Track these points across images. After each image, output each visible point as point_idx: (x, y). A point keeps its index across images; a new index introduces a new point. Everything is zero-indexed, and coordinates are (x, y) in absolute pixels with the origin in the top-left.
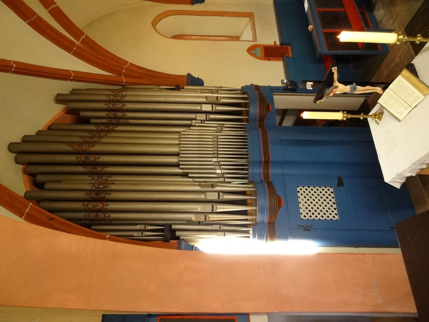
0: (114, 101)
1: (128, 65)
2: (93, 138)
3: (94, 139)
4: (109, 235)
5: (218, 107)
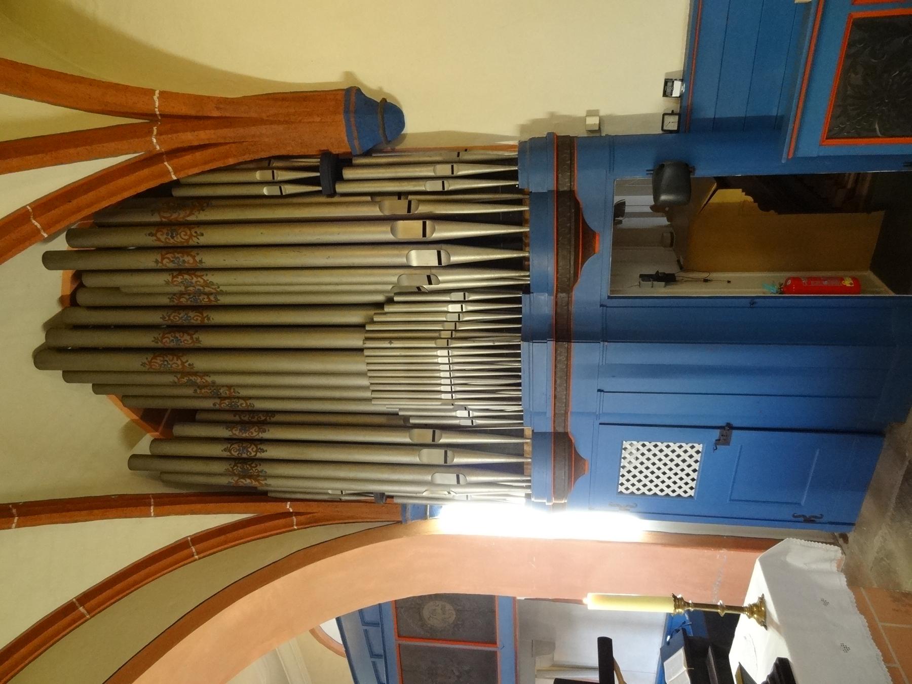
0: (181, 271)
1: (157, 104)
2: (181, 342)
3: (183, 343)
4: (289, 503)
5: (441, 275)
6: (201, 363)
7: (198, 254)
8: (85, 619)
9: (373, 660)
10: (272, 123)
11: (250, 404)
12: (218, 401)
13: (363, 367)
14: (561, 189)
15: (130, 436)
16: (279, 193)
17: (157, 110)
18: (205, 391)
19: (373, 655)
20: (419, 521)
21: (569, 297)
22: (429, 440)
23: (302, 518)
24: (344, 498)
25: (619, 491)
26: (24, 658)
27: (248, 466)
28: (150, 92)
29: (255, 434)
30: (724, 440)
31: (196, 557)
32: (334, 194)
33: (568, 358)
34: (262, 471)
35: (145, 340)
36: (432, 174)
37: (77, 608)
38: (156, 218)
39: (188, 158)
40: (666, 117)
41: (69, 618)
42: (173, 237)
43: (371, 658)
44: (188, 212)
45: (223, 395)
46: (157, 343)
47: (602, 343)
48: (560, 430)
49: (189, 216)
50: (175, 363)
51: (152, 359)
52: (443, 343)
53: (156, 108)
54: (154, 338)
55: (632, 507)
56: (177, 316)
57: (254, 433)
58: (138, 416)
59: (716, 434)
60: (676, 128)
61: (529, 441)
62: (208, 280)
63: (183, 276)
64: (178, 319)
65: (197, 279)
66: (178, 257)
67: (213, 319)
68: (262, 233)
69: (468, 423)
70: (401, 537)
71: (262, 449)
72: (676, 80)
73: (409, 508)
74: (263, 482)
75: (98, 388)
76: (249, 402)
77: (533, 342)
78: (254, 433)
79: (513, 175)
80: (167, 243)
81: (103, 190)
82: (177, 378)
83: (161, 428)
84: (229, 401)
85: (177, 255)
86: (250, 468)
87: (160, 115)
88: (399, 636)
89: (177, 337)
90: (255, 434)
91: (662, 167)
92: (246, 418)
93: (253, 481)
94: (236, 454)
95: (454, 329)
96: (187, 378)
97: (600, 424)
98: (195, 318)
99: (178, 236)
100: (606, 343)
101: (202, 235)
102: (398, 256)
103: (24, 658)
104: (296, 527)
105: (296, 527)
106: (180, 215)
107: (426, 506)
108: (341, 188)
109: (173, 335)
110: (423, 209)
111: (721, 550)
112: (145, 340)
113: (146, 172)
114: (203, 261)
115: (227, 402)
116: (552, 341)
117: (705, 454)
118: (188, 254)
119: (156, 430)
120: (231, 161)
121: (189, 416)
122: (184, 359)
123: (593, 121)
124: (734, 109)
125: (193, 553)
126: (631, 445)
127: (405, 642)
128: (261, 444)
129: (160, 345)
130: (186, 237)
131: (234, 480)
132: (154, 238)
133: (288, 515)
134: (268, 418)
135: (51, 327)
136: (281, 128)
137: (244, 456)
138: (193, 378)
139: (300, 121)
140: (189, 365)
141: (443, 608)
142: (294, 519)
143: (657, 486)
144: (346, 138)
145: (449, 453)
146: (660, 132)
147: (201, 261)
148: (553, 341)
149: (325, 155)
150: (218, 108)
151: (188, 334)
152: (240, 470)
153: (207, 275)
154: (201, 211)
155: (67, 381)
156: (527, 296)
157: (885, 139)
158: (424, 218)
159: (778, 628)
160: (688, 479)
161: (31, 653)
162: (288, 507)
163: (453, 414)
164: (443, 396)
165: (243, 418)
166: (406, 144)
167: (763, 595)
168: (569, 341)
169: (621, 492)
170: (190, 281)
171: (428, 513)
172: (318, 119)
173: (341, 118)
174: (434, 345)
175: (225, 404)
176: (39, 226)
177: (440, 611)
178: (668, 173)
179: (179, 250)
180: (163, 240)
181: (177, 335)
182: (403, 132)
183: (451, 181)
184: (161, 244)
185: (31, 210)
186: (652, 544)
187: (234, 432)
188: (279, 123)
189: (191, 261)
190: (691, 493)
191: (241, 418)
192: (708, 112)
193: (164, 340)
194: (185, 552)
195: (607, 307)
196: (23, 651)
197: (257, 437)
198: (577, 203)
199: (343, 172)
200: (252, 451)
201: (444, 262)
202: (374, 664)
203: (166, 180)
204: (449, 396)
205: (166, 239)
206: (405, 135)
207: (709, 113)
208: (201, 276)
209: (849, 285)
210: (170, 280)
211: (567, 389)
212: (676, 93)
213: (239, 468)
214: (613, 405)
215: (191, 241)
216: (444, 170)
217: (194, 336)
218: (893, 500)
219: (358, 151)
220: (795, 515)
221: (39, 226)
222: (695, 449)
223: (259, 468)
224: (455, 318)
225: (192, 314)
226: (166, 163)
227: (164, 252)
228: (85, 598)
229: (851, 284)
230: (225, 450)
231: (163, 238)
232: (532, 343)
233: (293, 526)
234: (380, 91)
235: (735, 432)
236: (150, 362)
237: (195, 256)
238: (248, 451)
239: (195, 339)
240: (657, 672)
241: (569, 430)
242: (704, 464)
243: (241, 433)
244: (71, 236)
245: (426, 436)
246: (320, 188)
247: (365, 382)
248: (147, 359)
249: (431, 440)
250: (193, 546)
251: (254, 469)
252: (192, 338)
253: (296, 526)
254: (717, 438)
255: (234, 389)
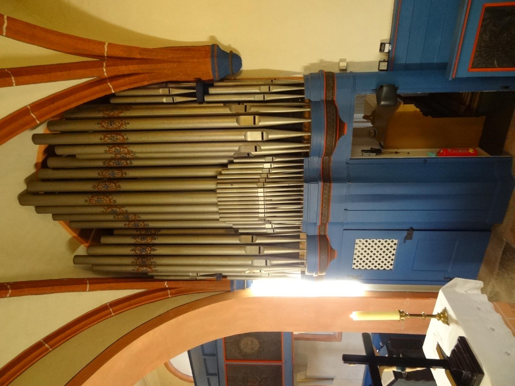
0: (114, 145)
1: (106, 50)
2: (109, 187)
3: (110, 188)
4: (166, 282)
5: (262, 146)
6: (120, 200)
7: (125, 135)
8: (48, 351)
9: (208, 377)
10: (171, 62)
11: (146, 224)
12: (127, 223)
13: (215, 200)
14: (327, 99)
15: (72, 245)
16: (172, 101)
17: (105, 53)
18: (120, 217)
19: (208, 374)
20: (240, 290)
21: (330, 159)
22: (250, 241)
23: (173, 291)
24: (198, 278)
25: (353, 268)
26: (14, 374)
27: (145, 259)
28: (103, 44)
29: (149, 241)
30: (409, 237)
31: (113, 314)
32: (203, 102)
33: (329, 192)
34: (153, 262)
35: (88, 187)
36: (258, 91)
37: (44, 345)
38: (101, 115)
39: (121, 81)
40: (381, 63)
41: (38, 351)
42: (111, 125)
43: (207, 375)
44: (120, 111)
45: (131, 219)
46: (95, 188)
47: (348, 183)
48: (322, 233)
49: (120, 113)
50: (105, 200)
51: (92, 197)
52: (261, 185)
53: (105, 52)
54: (93, 185)
55: (359, 276)
56: (107, 173)
57: (149, 240)
58: (76, 234)
59: (405, 233)
60: (386, 69)
61: (305, 240)
62: (130, 150)
63: (115, 148)
64: (107, 174)
65: (124, 149)
66: (113, 136)
67: (128, 174)
68: (163, 123)
69: (271, 231)
70: (231, 299)
71: (155, 249)
72: (386, 43)
73: (235, 282)
74: (154, 269)
75: (56, 217)
76: (145, 223)
77: (311, 183)
78: (149, 240)
79: (301, 92)
80: (107, 128)
81: (72, 98)
82: (105, 209)
83: (90, 242)
84: (134, 222)
85: (113, 135)
86: (146, 260)
87: (107, 57)
88: (226, 360)
89: (107, 185)
90: (149, 241)
91: (382, 87)
92: (143, 232)
93: (148, 268)
94: (138, 252)
95: (266, 177)
96: (111, 209)
97: (344, 230)
98: (118, 174)
99: (114, 124)
100: (350, 183)
101: (128, 123)
102: (240, 135)
103: (14, 374)
104: (170, 296)
105: (170, 296)
106: (115, 113)
107: (244, 281)
108: (207, 99)
109: (105, 184)
110: (253, 110)
111: (407, 299)
112: (88, 187)
113: (97, 88)
114: (128, 138)
115: (132, 223)
116: (321, 182)
117: (399, 245)
118: (120, 135)
119: (87, 243)
120: (146, 83)
121: (110, 232)
122: (110, 198)
123: (343, 65)
124: (415, 59)
125: (111, 312)
126: (360, 241)
127: (228, 363)
128: (153, 246)
129: (96, 189)
130: (119, 125)
131: (136, 268)
132: (100, 125)
133: (166, 289)
134: (156, 232)
135: (29, 181)
136: (175, 65)
137: (144, 253)
138: (114, 209)
139: (186, 62)
140: (114, 201)
141: (252, 341)
142: (169, 291)
143: (373, 264)
144: (211, 72)
145: (262, 248)
146: (377, 70)
147: (127, 139)
148: (322, 182)
149: (198, 81)
150: (140, 54)
151: (114, 183)
152: (141, 261)
153: (129, 147)
154: (128, 111)
155: (38, 213)
156: (307, 158)
157: (499, 68)
158: (254, 114)
159: (456, 322)
160: (389, 260)
161: (18, 371)
162: (166, 284)
163: (263, 226)
164: (260, 215)
165: (141, 232)
166: (242, 76)
167: (445, 308)
168: (330, 182)
169: (354, 268)
170: (119, 150)
171: (245, 286)
172: (196, 60)
173: (209, 60)
174: (256, 186)
175: (132, 225)
176: (34, 117)
177: (250, 343)
178: (385, 89)
179: (114, 132)
180: (105, 127)
181: (107, 184)
182: (241, 69)
183: (268, 95)
184: (103, 129)
185: (30, 108)
186: (370, 297)
187: (137, 240)
188: (174, 62)
189: (121, 138)
190: (391, 267)
191: (140, 232)
192: (402, 59)
193: (99, 187)
194: (107, 312)
195: (349, 164)
196: (13, 370)
197: (151, 243)
198: (336, 107)
199: (209, 90)
200: (148, 251)
201: (265, 139)
202: (208, 379)
203: (107, 93)
204: (263, 215)
205: (107, 126)
206: (242, 71)
207: (403, 62)
208: (126, 148)
209: (472, 152)
210: (108, 150)
211: (328, 209)
212: (386, 50)
213: (140, 261)
214: (352, 217)
215: (122, 127)
216: (265, 89)
217: (117, 184)
218: (498, 265)
219: (217, 79)
220: (446, 277)
221: (34, 117)
222: (394, 243)
223: (152, 261)
224: (267, 171)
225: (116, 172)
226: (109, 84)
227: (105, 134)
228: (48, 339)
229: (473, 151)
230: (132, 250)
231: (105, 125)
232: (310, 184)
233: (168, 296)
234: (229, 47)
235: (415, 232)
236: (90, 200)
237: (124, 136)
238: (146, 251)
239: (117, 186)
240: (363, 379)
241: (327, 234)
242: (398, 250)
243: (141, 241)
244: (50, 124)
245: (248, 239)
246: (195, 99)
247: (215, 209)
248: (88, 197)
249: (251, 241)
250: (111, 308)
251: (149, 261)
252: (115, 185)
253: (170, 295)
254: (406, 236)
255: (138, 215)
